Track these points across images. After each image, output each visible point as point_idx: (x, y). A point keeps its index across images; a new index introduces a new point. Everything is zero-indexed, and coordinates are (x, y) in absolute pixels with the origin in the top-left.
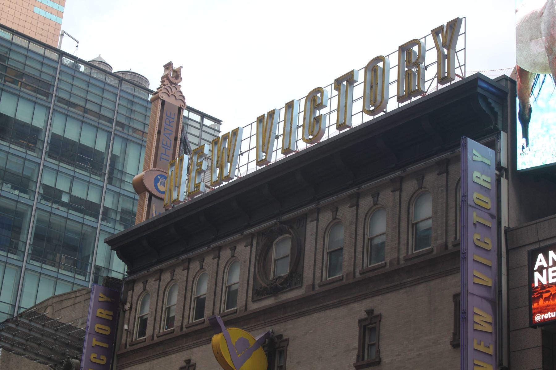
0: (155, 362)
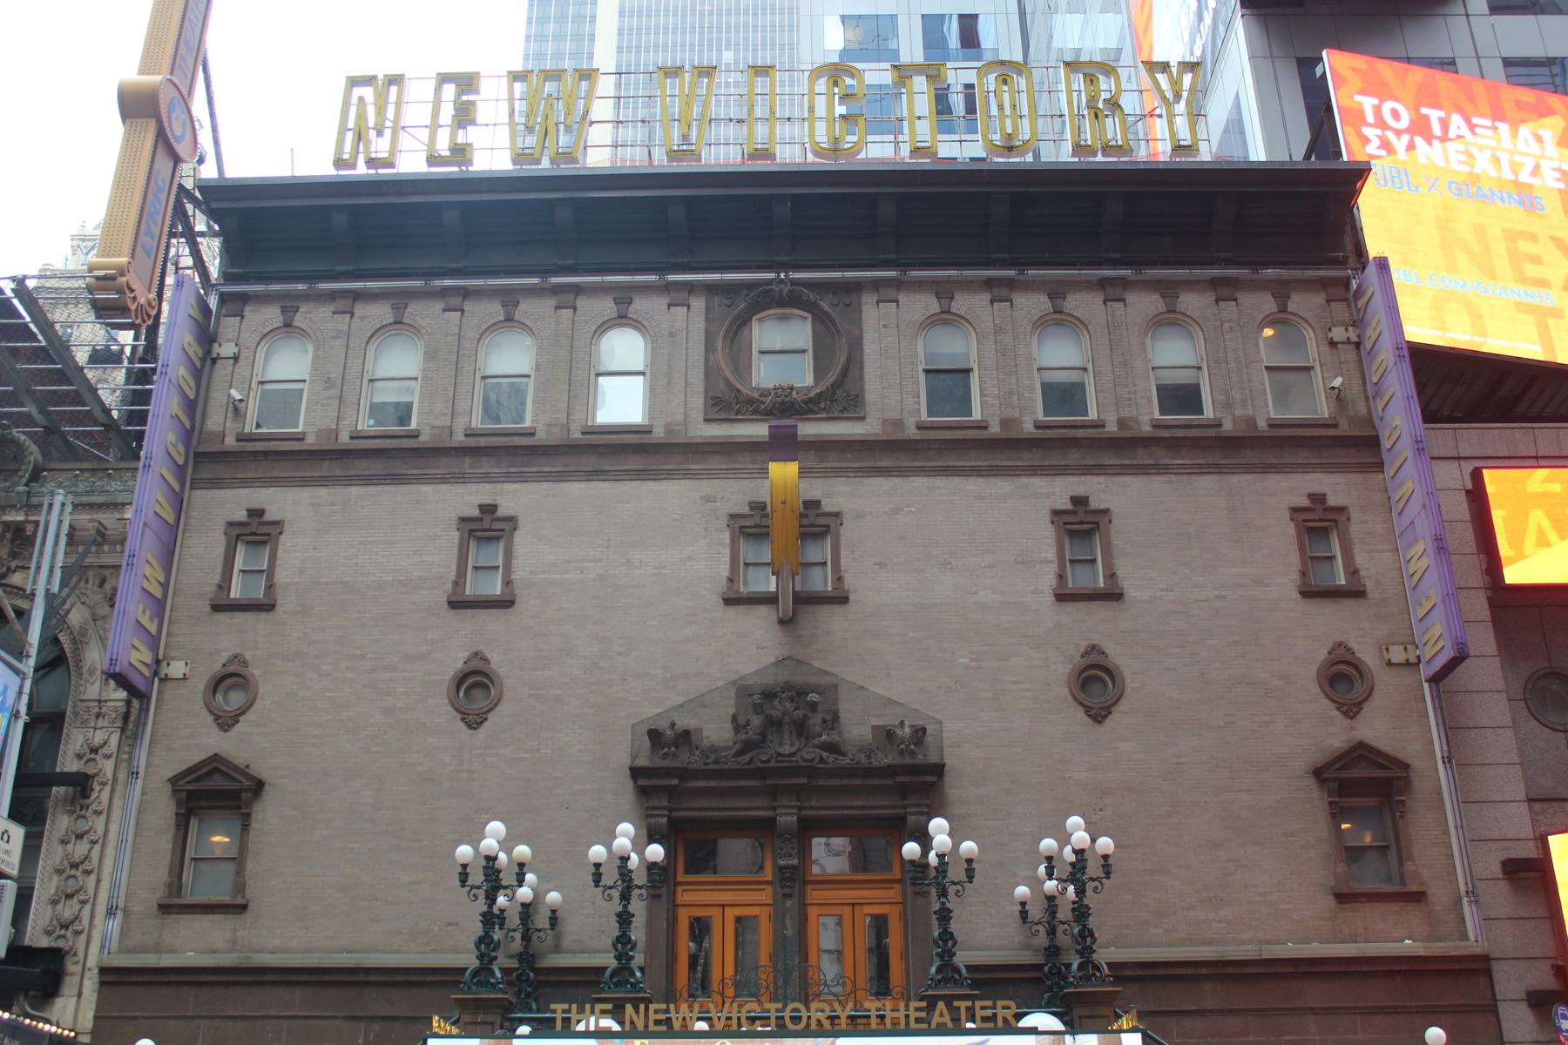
0: (355, 491)
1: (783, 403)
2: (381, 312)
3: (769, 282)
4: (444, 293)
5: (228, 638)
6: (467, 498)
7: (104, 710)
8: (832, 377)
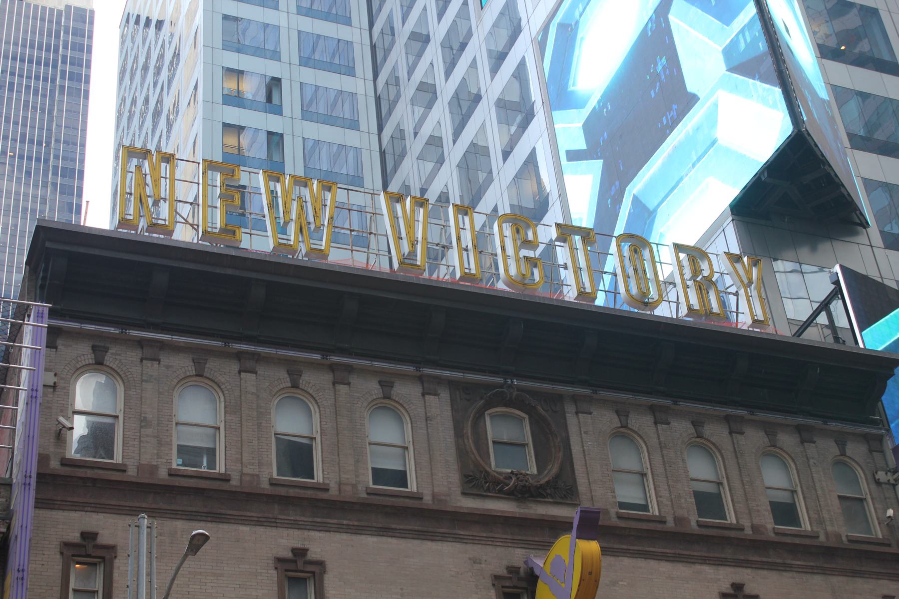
1: (524, 486)
2: (183, 364)
3: (501, 386)
6: (283, 541)
8: (553, 469)
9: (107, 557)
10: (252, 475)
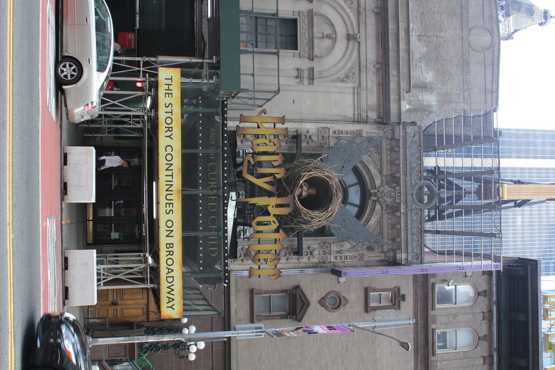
2: (483, 330)
4: (491, 356)
5: (354, 297)
7: (327, 254)
9: (395, 306)
10: (436, 366)
